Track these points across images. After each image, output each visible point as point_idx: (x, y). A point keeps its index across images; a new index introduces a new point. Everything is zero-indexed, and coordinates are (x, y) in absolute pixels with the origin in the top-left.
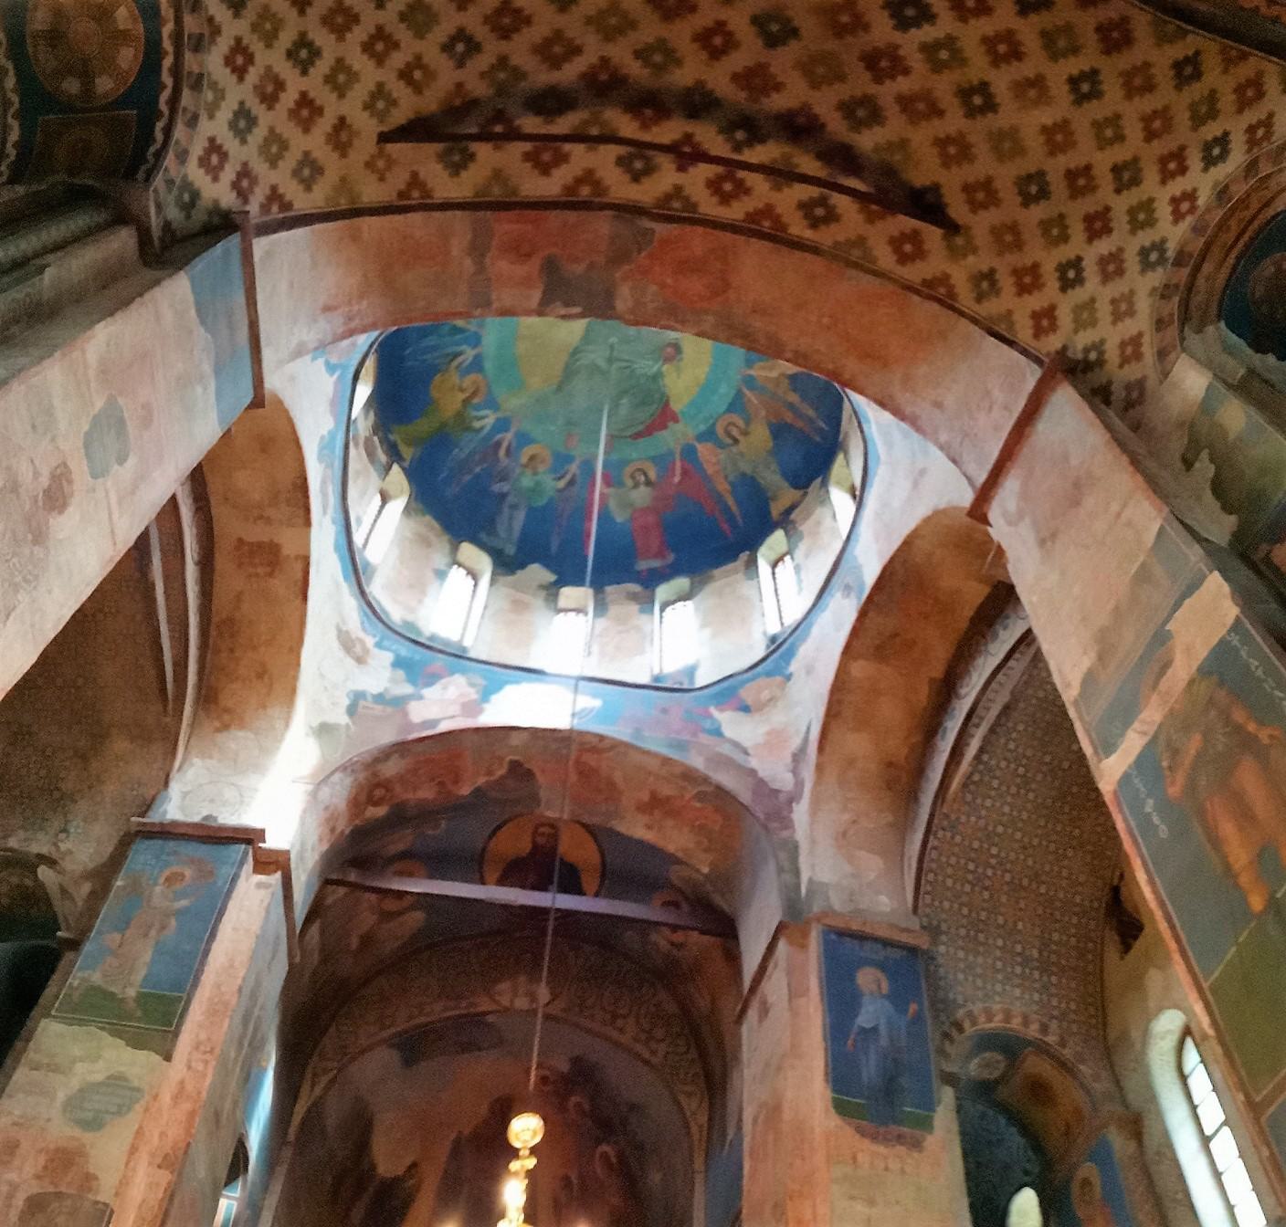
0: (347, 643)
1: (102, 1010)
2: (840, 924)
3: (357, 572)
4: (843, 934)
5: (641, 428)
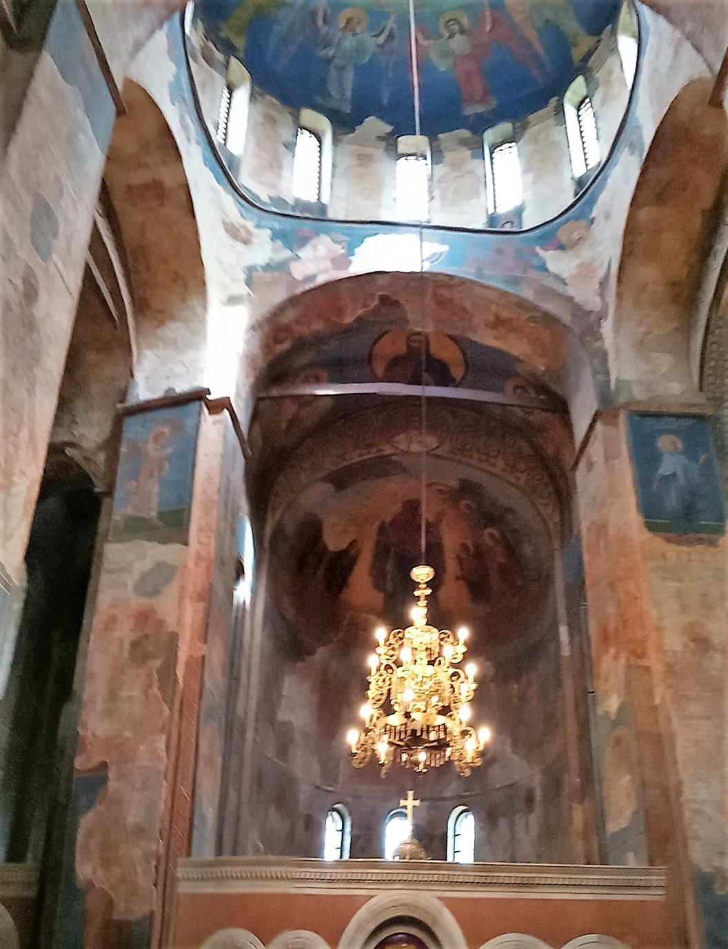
0: (233, 231)
1: (138, 528)
2: (642, 408)
3: (224, 167)
4: (645, 415)
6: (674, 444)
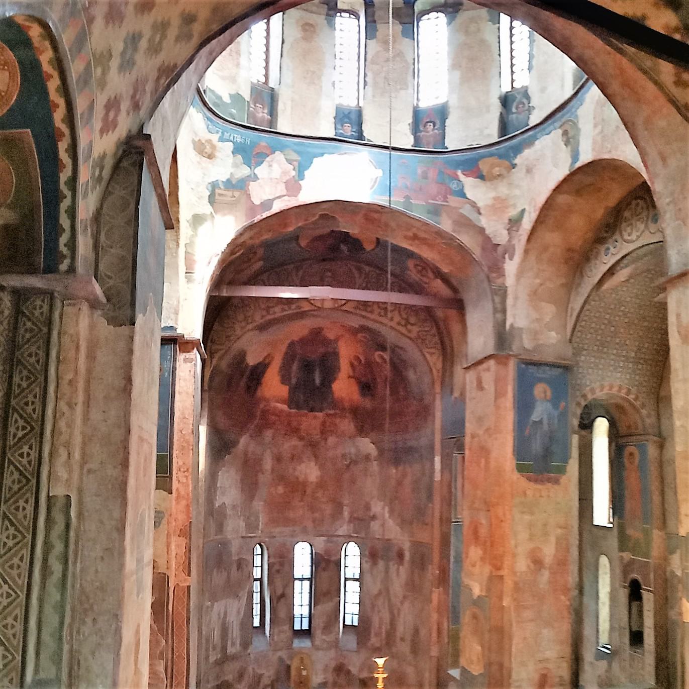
6: (545, 392)
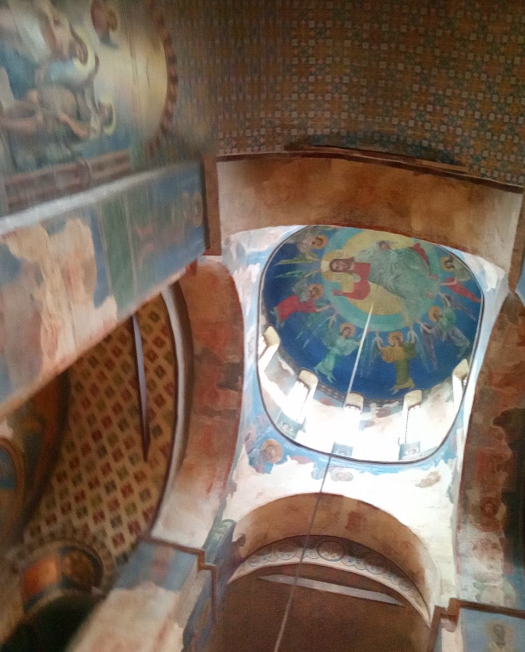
5: (424, 261)
